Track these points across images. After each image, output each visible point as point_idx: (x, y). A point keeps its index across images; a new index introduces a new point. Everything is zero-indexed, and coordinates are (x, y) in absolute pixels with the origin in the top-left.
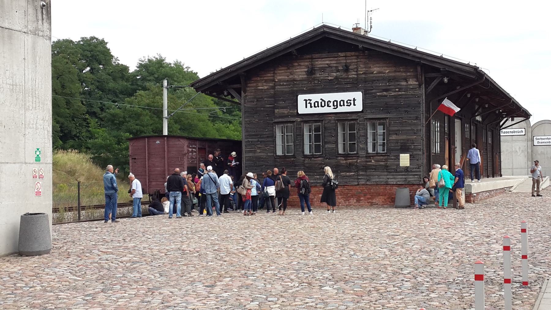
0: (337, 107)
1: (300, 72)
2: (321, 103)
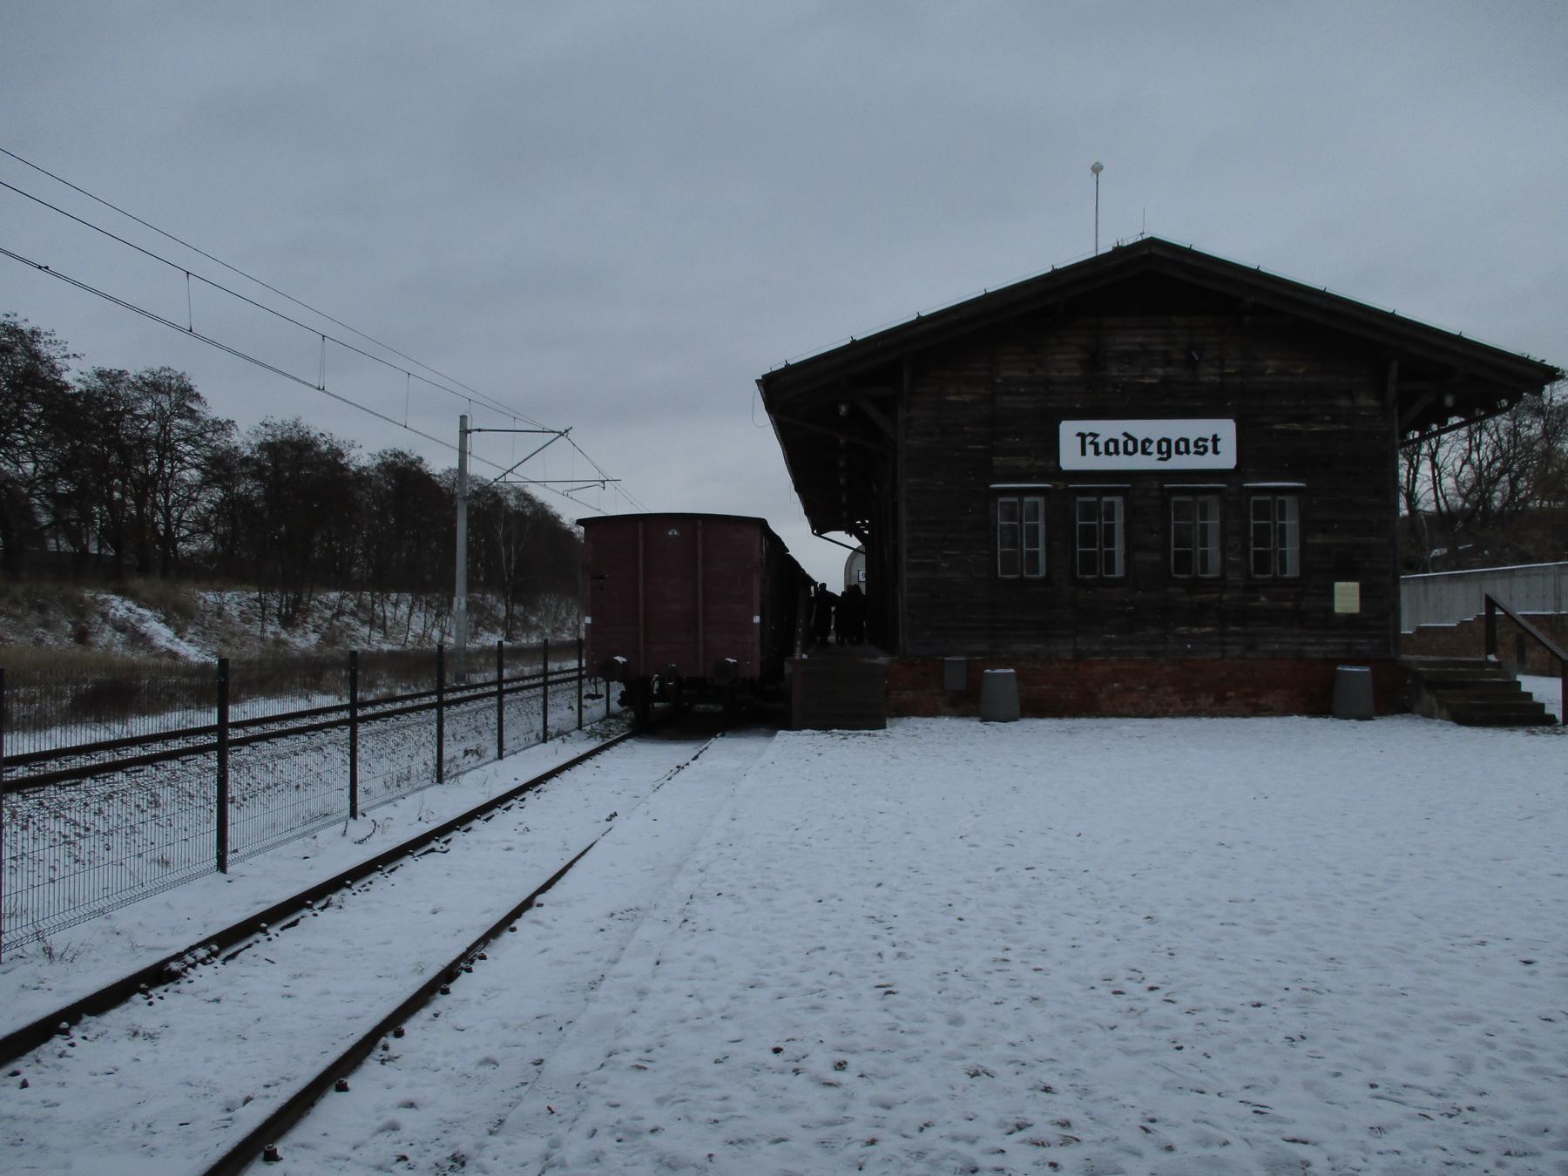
0: (1169, 456)
1: (1065, 363)
2: (1125, 444)
